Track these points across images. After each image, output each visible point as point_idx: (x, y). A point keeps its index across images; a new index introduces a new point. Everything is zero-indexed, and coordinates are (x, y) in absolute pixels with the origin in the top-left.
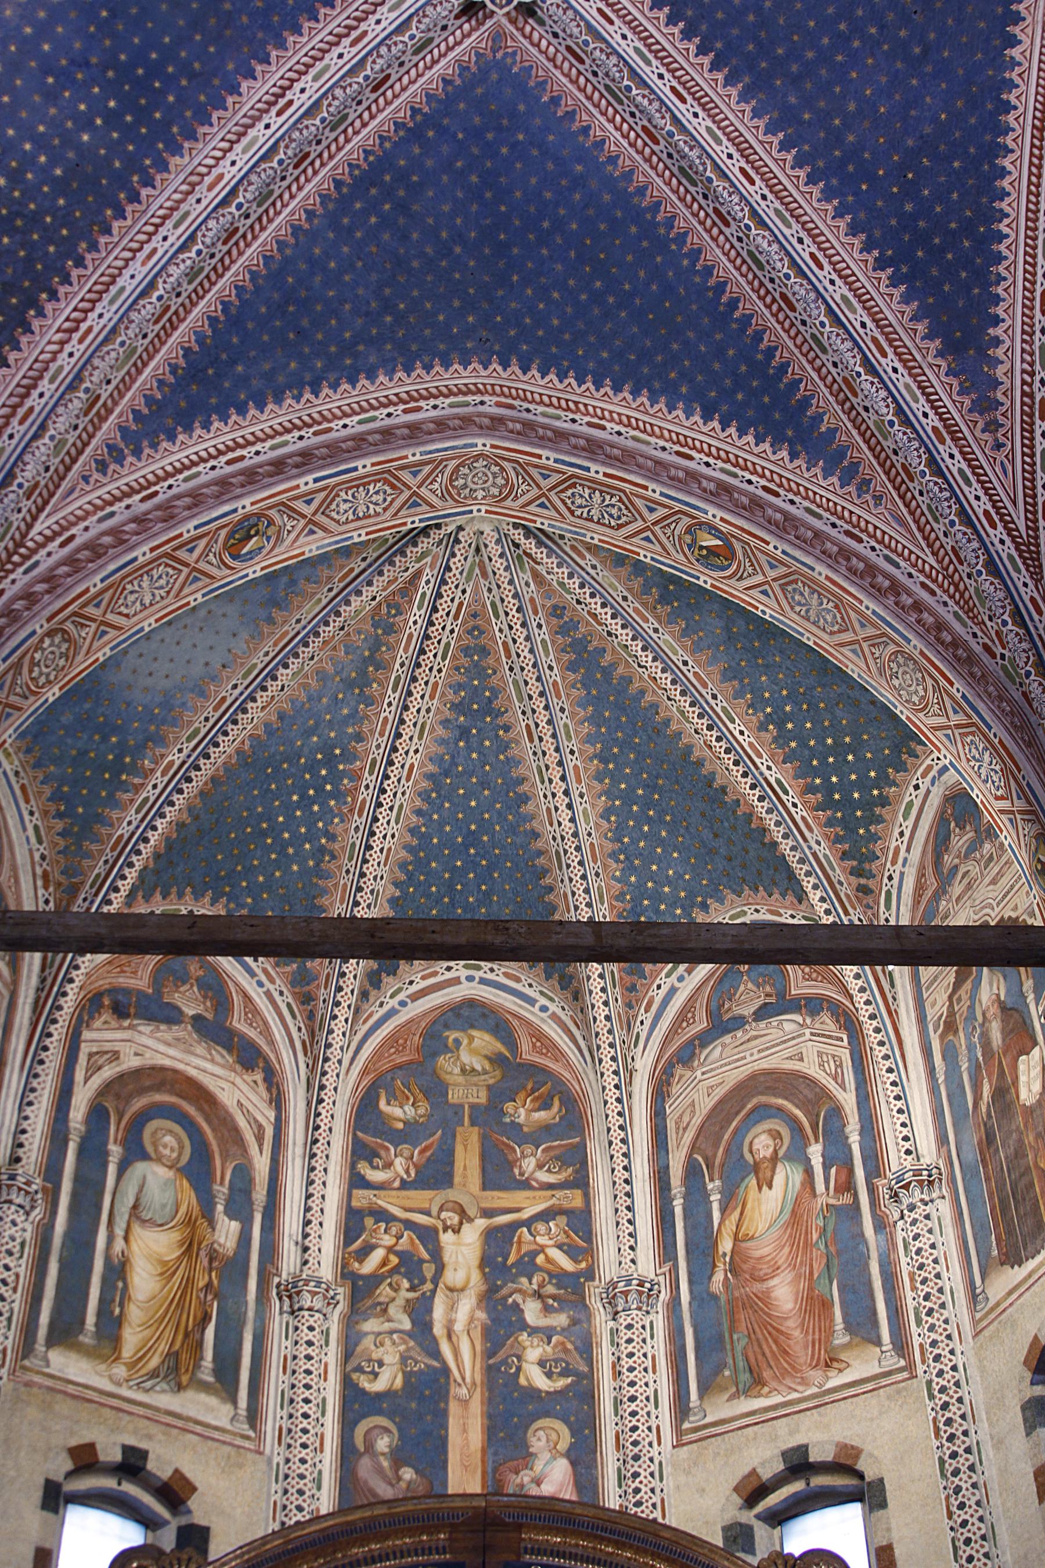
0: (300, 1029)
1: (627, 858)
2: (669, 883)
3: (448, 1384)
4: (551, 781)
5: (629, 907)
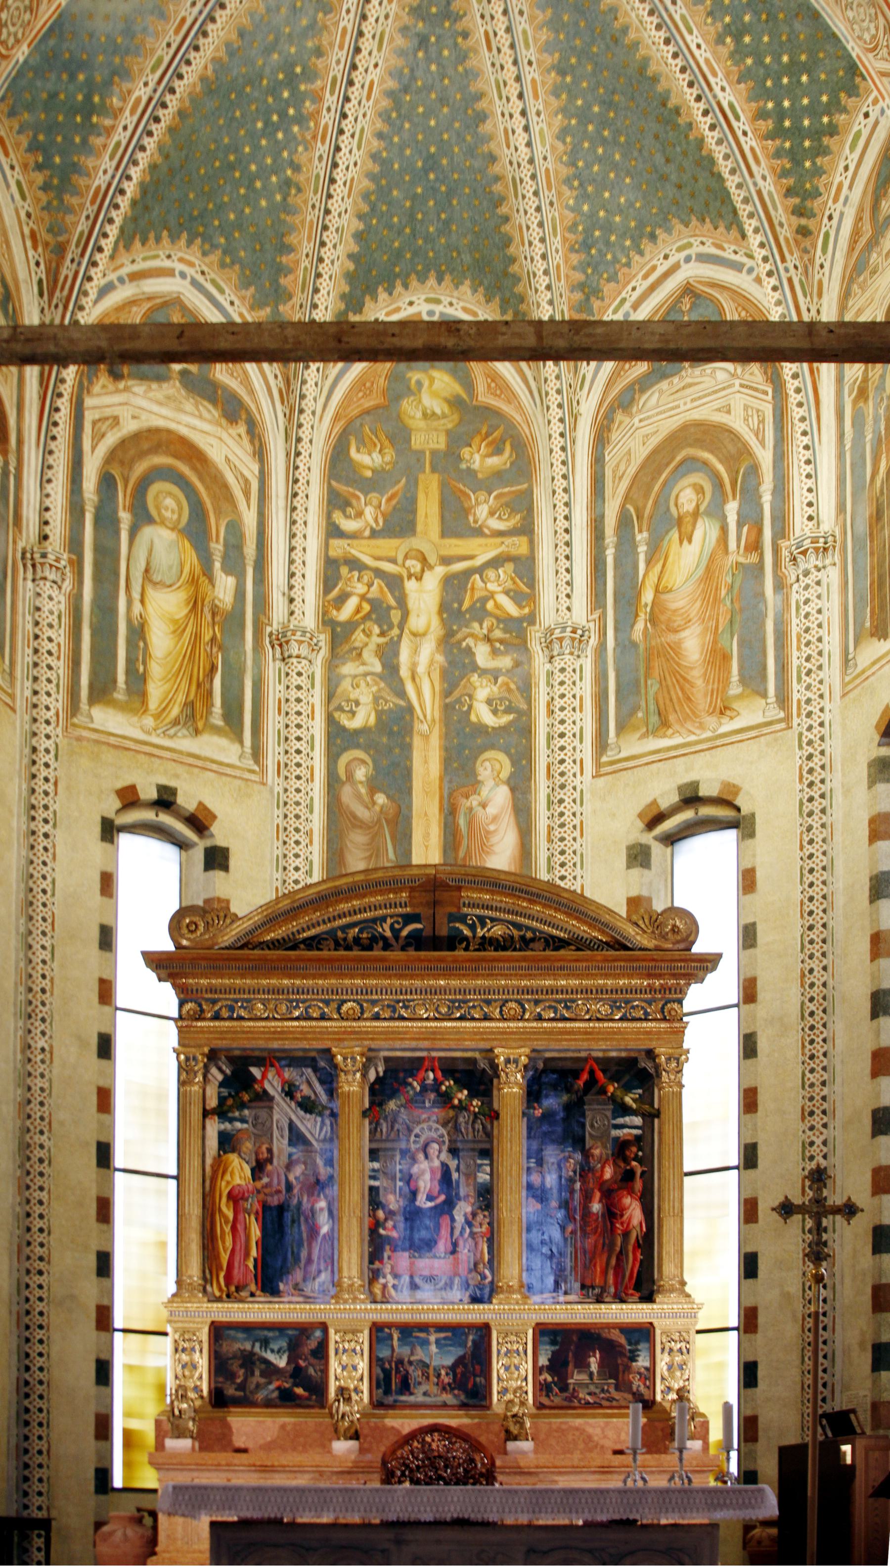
0: (276, 377)
1: (581, 185)
2: (621, 212)
3: (412, 721)
4: (508, 100)
5: (581, 239)
